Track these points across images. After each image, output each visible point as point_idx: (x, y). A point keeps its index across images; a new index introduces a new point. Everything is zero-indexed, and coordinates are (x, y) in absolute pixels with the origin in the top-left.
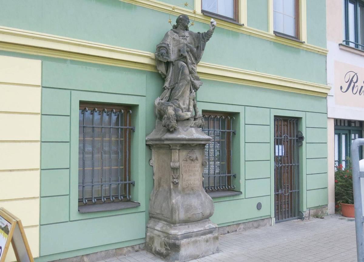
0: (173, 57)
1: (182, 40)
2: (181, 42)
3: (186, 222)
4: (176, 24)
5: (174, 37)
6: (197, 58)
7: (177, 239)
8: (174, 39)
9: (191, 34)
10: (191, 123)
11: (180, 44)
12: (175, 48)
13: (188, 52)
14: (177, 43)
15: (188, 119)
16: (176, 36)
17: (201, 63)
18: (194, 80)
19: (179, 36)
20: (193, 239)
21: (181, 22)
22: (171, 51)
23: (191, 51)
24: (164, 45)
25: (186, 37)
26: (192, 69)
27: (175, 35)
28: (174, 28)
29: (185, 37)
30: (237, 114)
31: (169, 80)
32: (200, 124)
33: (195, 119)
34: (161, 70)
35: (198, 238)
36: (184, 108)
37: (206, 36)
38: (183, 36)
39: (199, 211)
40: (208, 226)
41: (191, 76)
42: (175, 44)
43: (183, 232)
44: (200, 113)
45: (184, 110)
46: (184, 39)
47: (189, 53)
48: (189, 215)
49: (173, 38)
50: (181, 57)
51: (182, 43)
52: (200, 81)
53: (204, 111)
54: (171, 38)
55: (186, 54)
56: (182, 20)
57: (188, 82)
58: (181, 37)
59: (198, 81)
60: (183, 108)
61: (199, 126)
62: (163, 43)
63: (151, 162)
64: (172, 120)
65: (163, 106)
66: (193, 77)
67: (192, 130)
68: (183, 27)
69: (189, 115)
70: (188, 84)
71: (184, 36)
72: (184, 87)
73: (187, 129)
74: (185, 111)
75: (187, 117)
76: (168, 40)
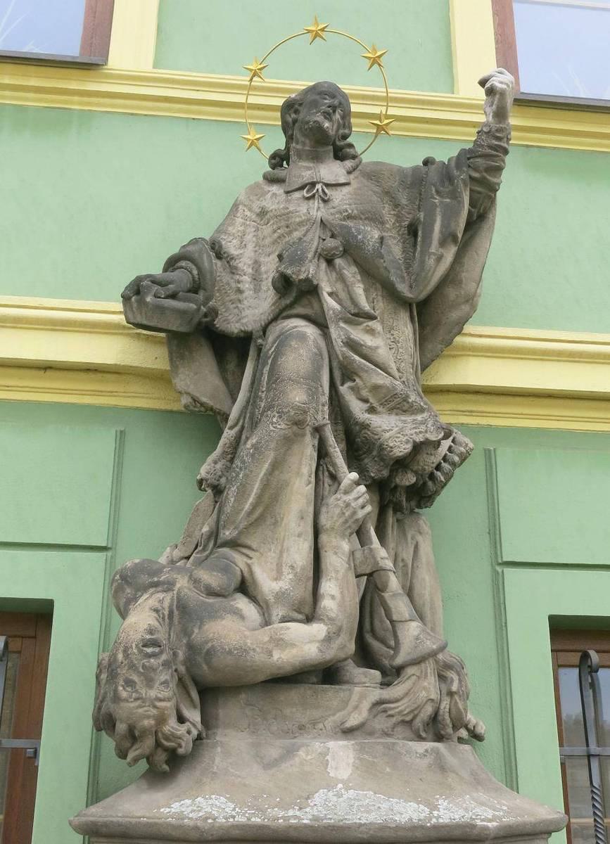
1: (303, 208)
2: (297, 220)
5: (264, 203)
8: (263, 213)
9: (374, 174)
10: (346, 703)
11: (290, 233)
12: (271, 257)
13: (330, 262)
14: (275, 231)
17: (476, 332)
18: (372, 410)
19: (287, 193)
21: (295, 121)
22: (246, 278)
25: (327, 185)
26: (353, 345)
27: (269, 195)
28: (274, 167)
29: (319, 186)
32: (429, 710)
34: (192, 390)
36: (280, 596)
38: (302, 188)
41: (352, 388)
42: (268, 241)
45: (278, 612)
46: (308, 199)
47: (338, 261)
49: (258, 211)
51: (301, 224)
52: (419, 417)
54: (248, 213)
55: (313, 270)
56: (296, 112)
58: (297, 195)
59: (409, 418)
60: (271, 599)
61: (418, 723)
64: (129, 683)
65: (128, 590)
66: (365, 393)
67: (324, 754)
68: (307, 141)
70: (298, 436)
71: (313, 184)
72: (270, 456)
73: (289, 753)
74: (285, 620)
76: (233, 224)
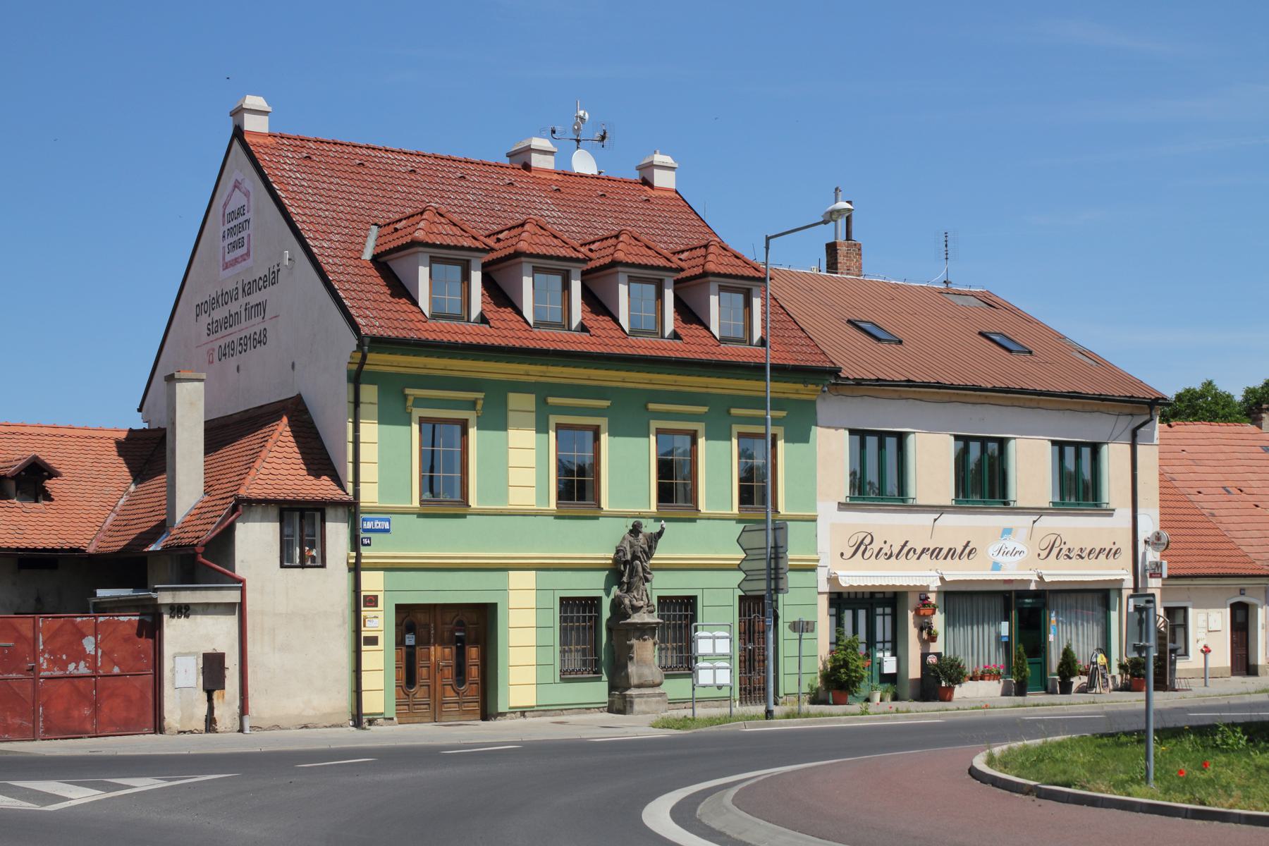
0: (629, 557)
3: (639, 686)
4: (631, 528)
6: (649, 558)
7: (632, 697)
15: (642, 607)
16: (631, 539)
20: (644, 699)
23: (645, 551)
24: (621, 548)
30: (695, 598)
31: (626, 575)
33: (648, 606)
35: (649, 699)
37: (660, 534)
39: (651, 679)
40: (657, 690)
43: (637, 693)
44: (655, 601)
48: (642, 681)
50: (635, 557)
53: (659, 598)
55: (640, 554)
57: (640, 580)
62: (621, 546)
63: (613, 642)
69: (641, 603)
75: (640, 605)
